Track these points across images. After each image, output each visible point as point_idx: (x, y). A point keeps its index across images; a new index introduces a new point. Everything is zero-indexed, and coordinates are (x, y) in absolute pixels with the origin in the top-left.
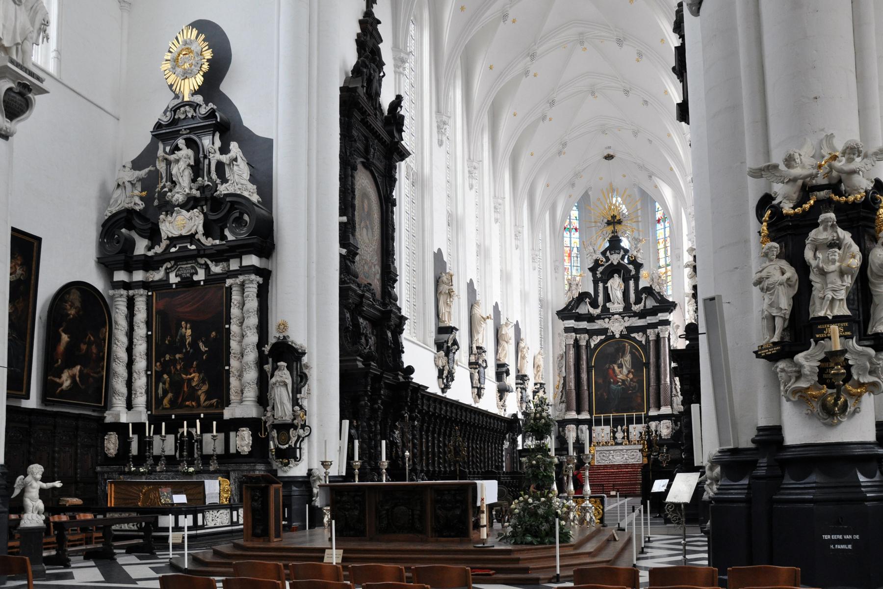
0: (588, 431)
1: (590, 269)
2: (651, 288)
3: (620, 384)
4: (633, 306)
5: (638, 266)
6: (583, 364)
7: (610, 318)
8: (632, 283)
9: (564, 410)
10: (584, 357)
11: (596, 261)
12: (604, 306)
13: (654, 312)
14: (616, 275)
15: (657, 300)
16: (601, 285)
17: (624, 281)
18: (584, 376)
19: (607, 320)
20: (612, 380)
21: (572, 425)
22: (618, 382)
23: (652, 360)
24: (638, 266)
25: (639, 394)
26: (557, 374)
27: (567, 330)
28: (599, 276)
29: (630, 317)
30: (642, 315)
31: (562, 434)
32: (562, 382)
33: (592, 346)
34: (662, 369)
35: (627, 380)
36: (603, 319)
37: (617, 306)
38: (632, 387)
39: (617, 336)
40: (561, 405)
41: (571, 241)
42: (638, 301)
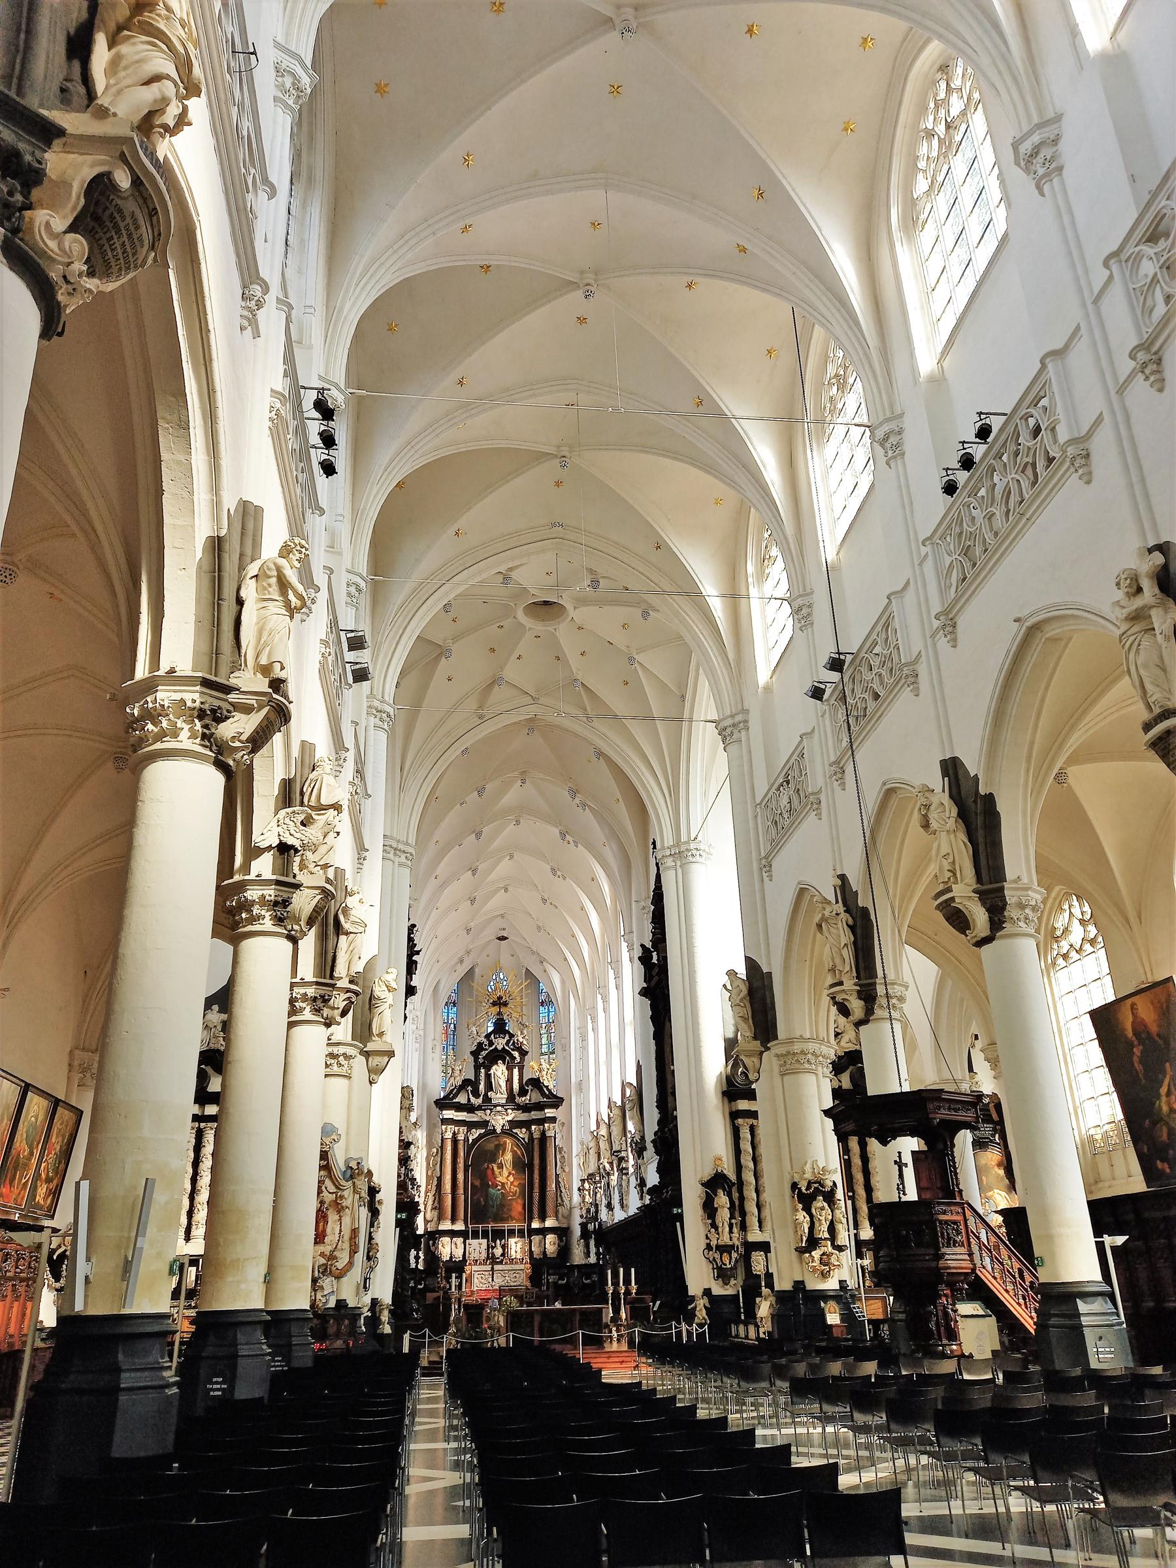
1: (472, 1053)
2: (538, 1080)
4: (517, 1098)
5: (523, 1053)
7: (491, 1110)
8: (516, 1071)
9: (436, 1219)
10: (462, 1154)
11: (480, 1045)
12: (486, 1095)
13: (540, 1107)
15: (543, 1094)
16: (483, 1071)
17: (507, 1068)
18: (460, 1176)
19: (489, 1111)
23: (536, 1161)
24: (523, 1053)
26: (430, 1173)
27: (445, 1121)
28: (481, 1061)
29: (513, 1109)
30: (526, 1108)
31: (433, 1249)
32: (435, 1183)
33: (470, 1141)
34: (549, 1173)
36: (485, 1110)
37: (500, 1097)
39: (499, 1131)
41: (448, 1016)
42: (523, 1092)
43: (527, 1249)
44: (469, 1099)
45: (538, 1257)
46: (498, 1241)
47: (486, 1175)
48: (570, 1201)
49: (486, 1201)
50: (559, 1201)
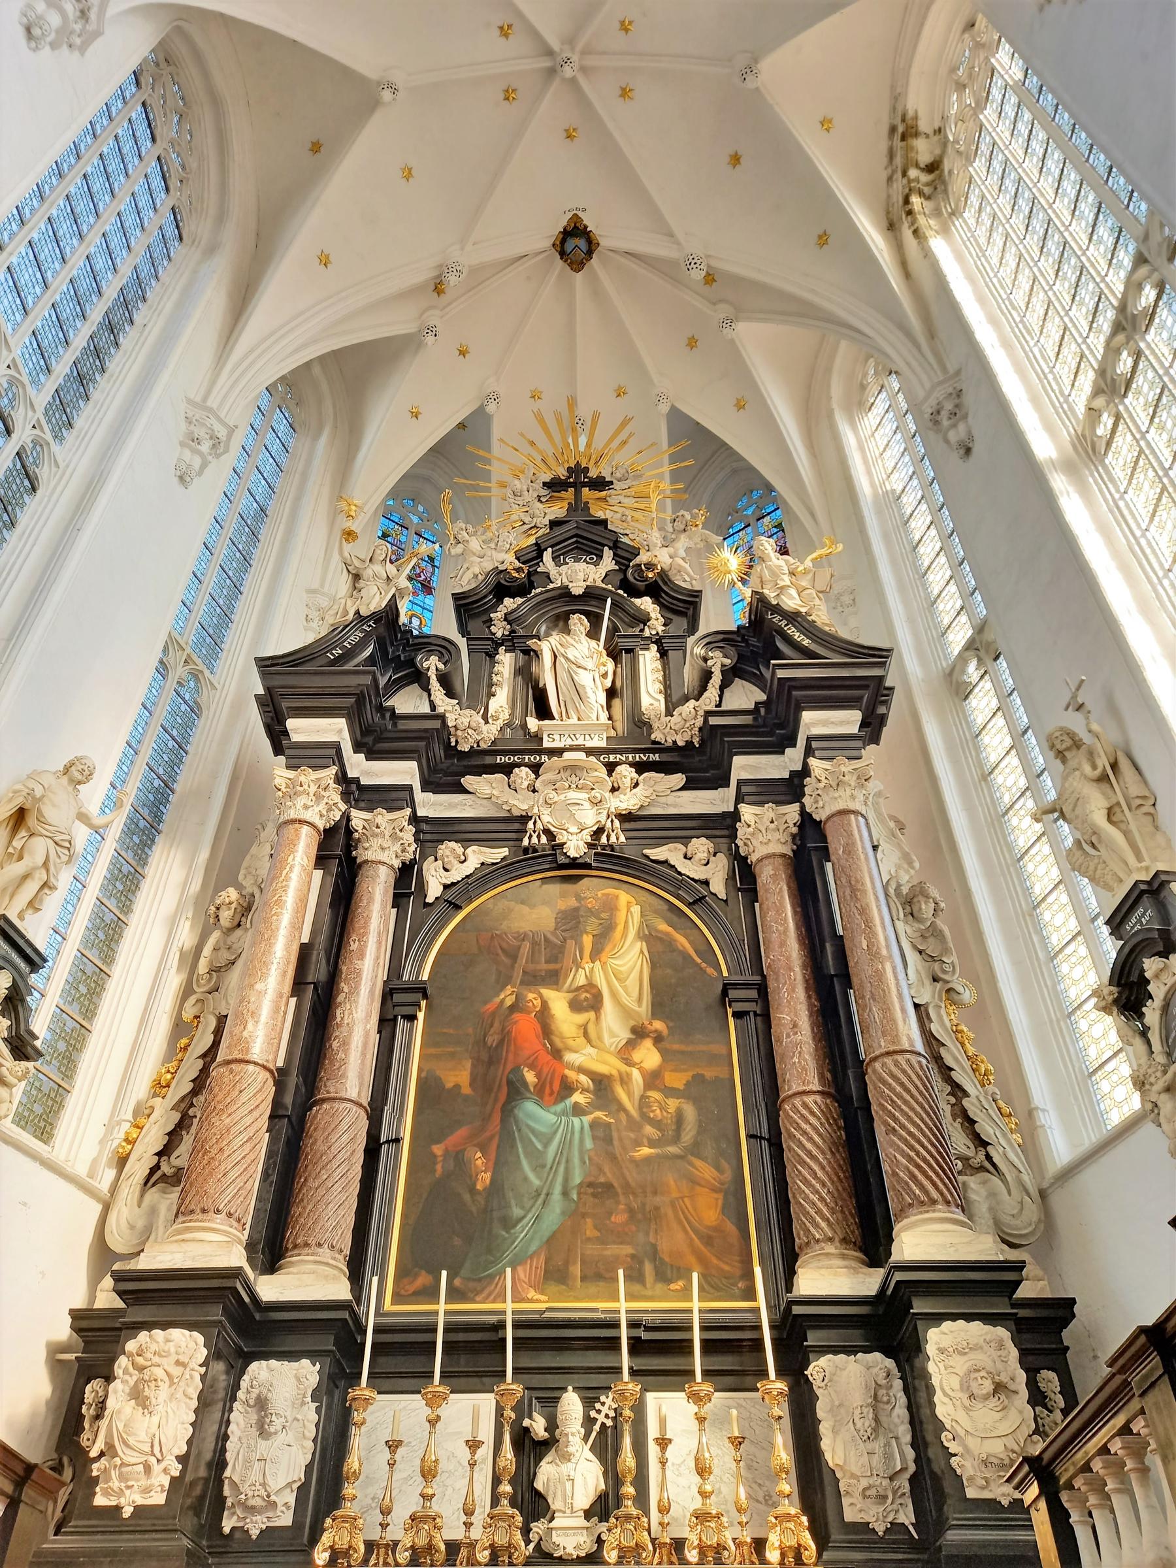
0: (310, 1415)
3: (578, 1097)
6: (362, 957)
7: (536, 768)
8: (649, 660)
14: (579, 623)
17: (614, 654)
19: (523, 775)
20: (530, 1077)
21: (177, 1334)
22: (567, 1088)
25: (705, 1171)
28: (500, 629)
29: (641, 768)
33: (434, 891)
35: (625, 1080)
36: (507, 770)
38: (657, 1124)
40: (153, 1194)
43: (783, 1452)
44: (433, 707)
45: (876, 1517)
46: (571, 1404)
47: (505, 1037)
48: (1031, 1147)
49: (502, 1163)
50: (960, 1142)
